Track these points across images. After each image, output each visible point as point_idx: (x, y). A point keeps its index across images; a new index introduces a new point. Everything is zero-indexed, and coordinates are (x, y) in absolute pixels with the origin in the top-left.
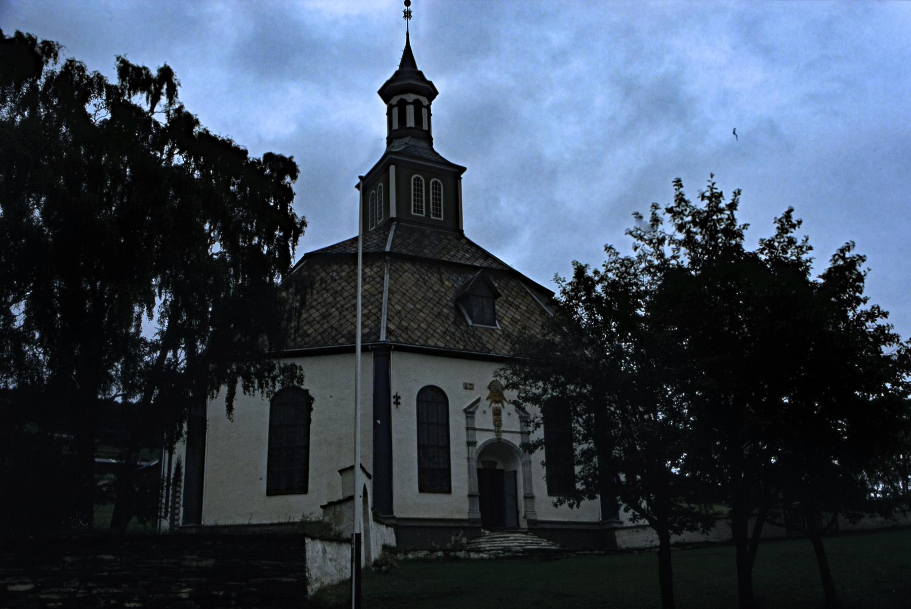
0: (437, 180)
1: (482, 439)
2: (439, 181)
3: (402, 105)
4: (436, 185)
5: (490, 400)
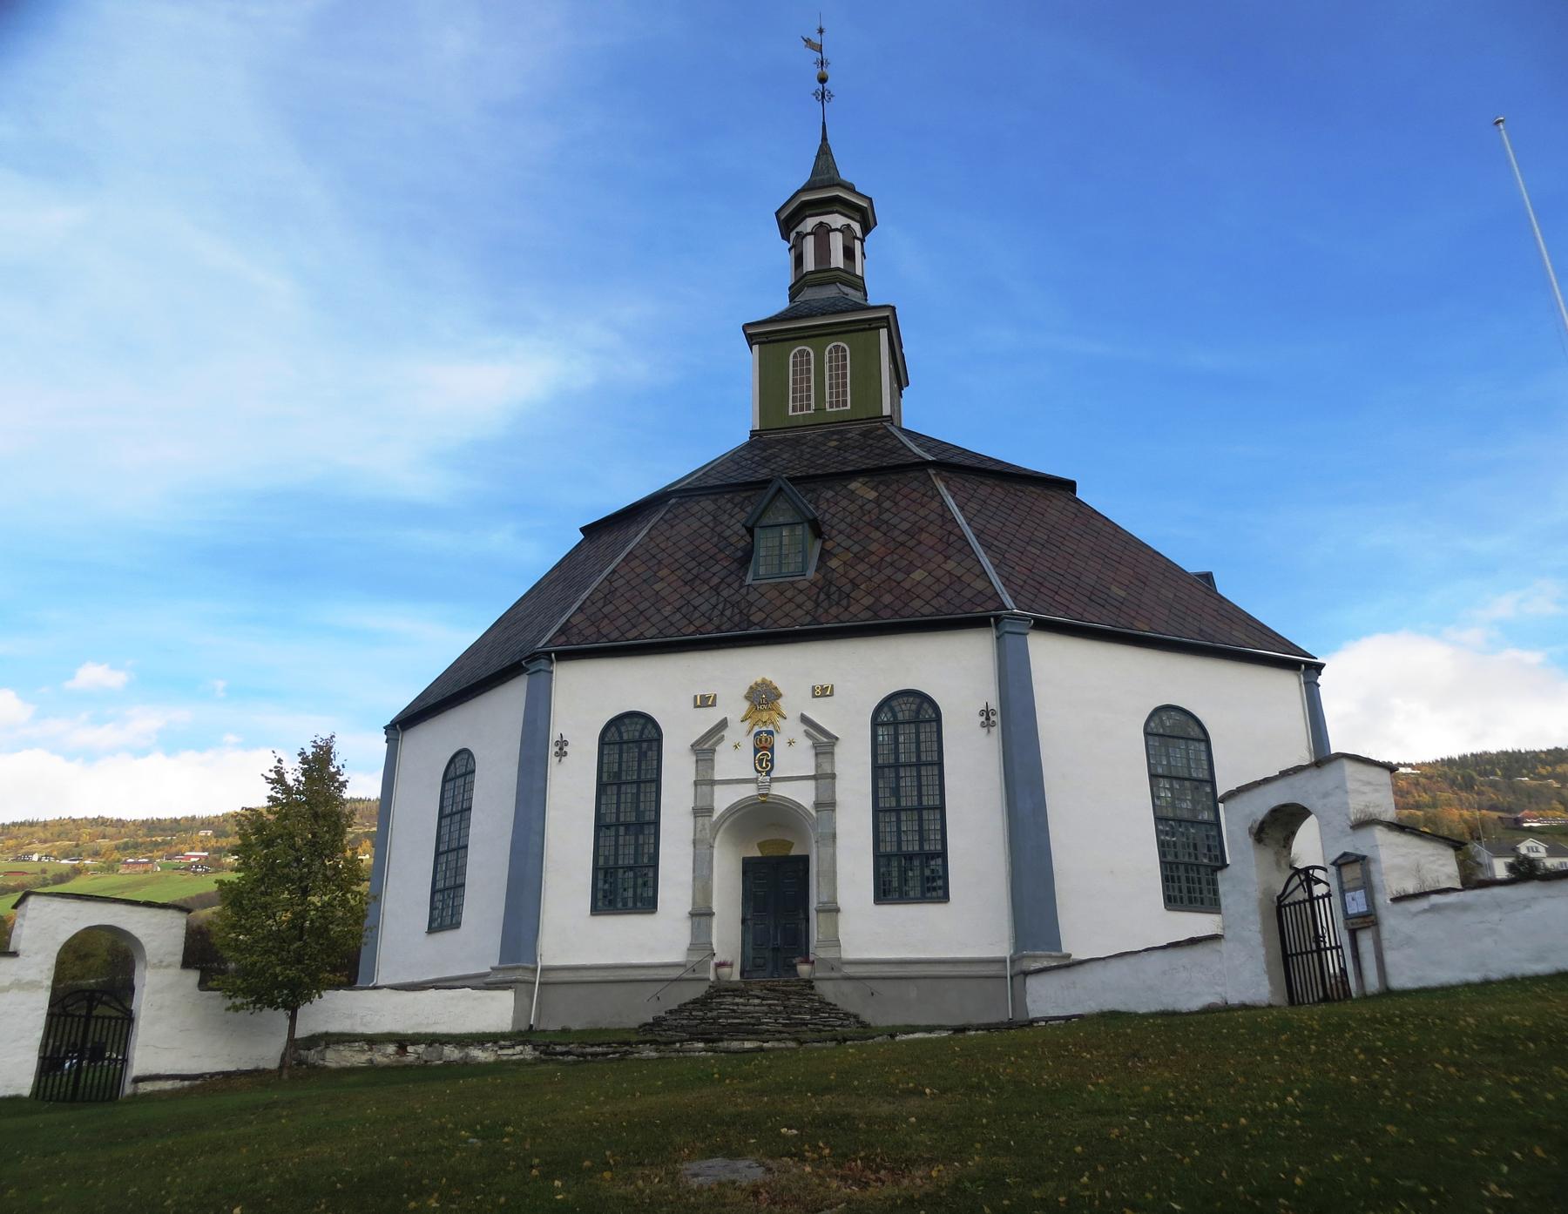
0: (839, 343)
1: (724, 799)
4: (837, 352)
5: (749, 721)
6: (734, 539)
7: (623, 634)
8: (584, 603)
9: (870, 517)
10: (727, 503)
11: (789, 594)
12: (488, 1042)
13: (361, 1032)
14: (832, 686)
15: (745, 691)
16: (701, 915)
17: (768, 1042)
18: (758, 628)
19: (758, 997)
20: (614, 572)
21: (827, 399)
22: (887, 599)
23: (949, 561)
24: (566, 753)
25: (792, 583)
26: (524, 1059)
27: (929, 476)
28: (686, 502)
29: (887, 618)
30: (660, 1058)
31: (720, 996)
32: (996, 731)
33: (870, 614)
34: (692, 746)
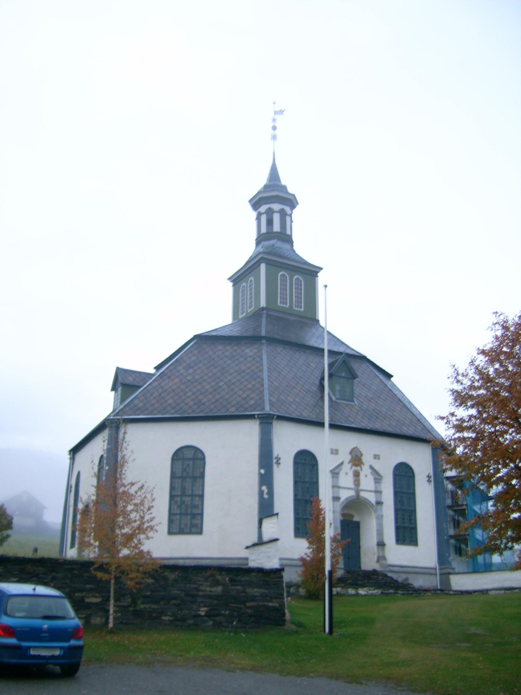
1: (345, 495)
3: (270, 212)
24: (279, 463)
34: (331, 471)
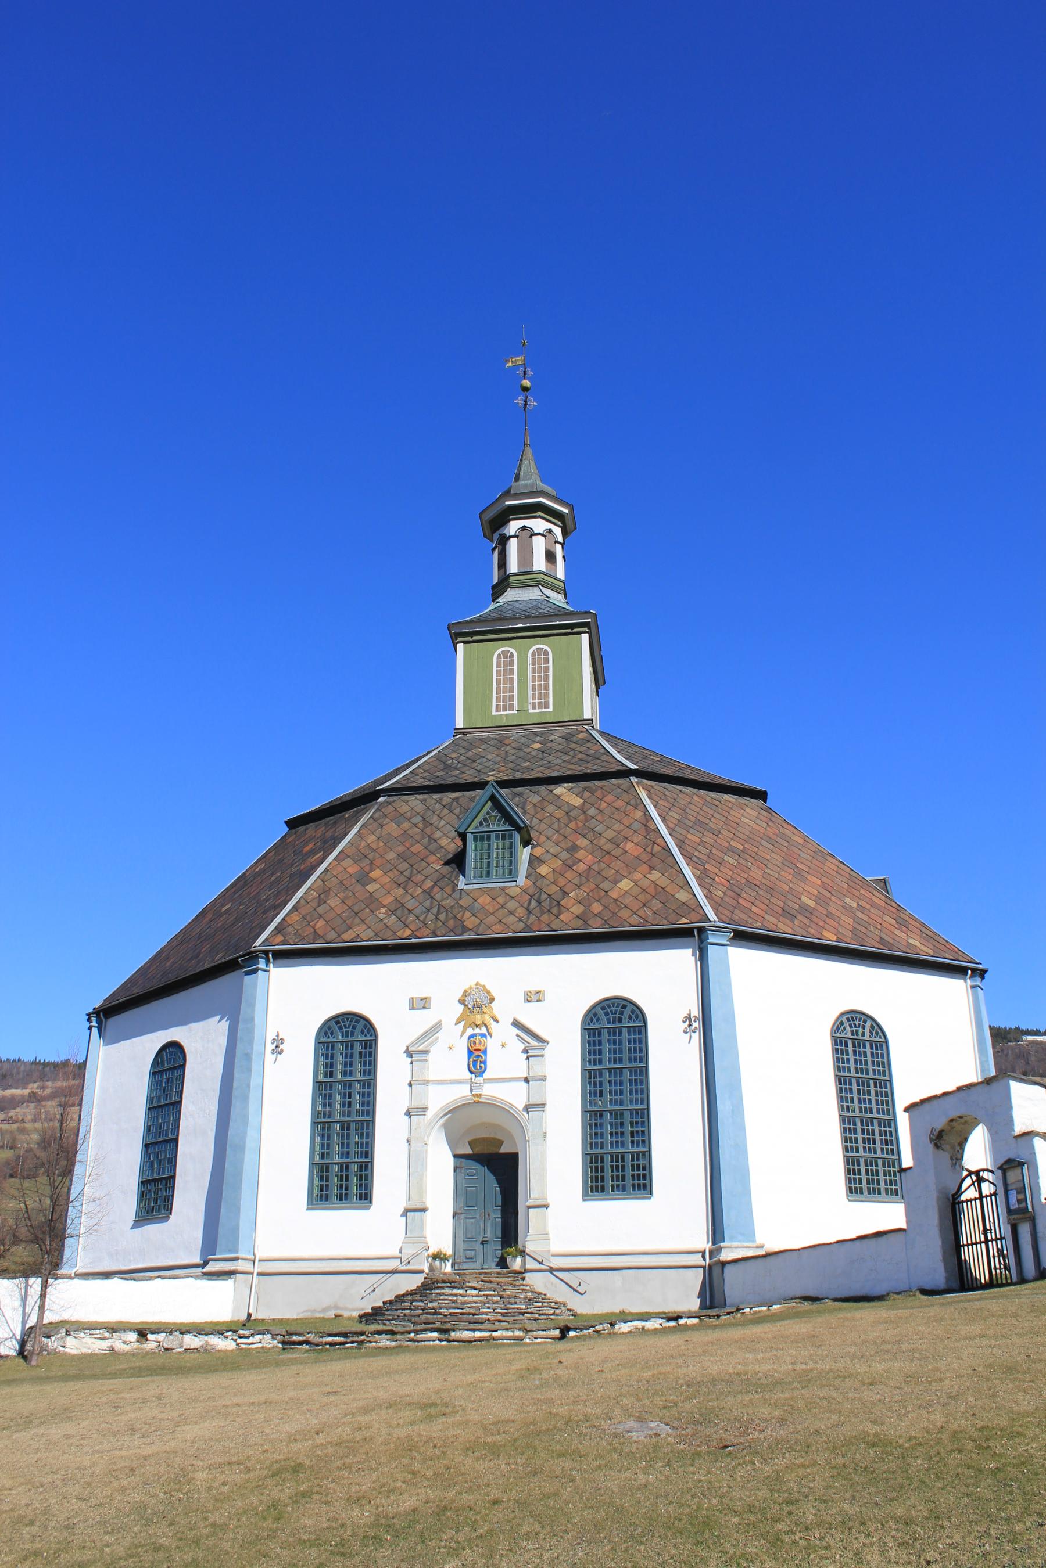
2: (545, 647)
5: (463, 1023)
6: (444, 842)
7: (339, 935)
8: (298, 902)
9: (576, 823)
10: (436, 804)
11: (501, 900)
12: (228, 1331)
13: (94, 1320)
14: (544, 991)
15: (460, 995)
16: (414, 1211)
17: (497, 1331)
18: (473, 933)
19: (475, 1289)
20: (326, 870)
21: (530, 701)
22: (596, 908)
23: (653, 872)
25: (503, 889)
26: (263, 1347)
27: (632, 783)
28: (394, 801)
29: (596, 927)
30: (397, 1347)
31: (438, 1288)
32: (697, 1037)
33: (580, 922)
